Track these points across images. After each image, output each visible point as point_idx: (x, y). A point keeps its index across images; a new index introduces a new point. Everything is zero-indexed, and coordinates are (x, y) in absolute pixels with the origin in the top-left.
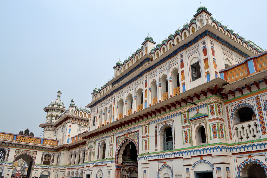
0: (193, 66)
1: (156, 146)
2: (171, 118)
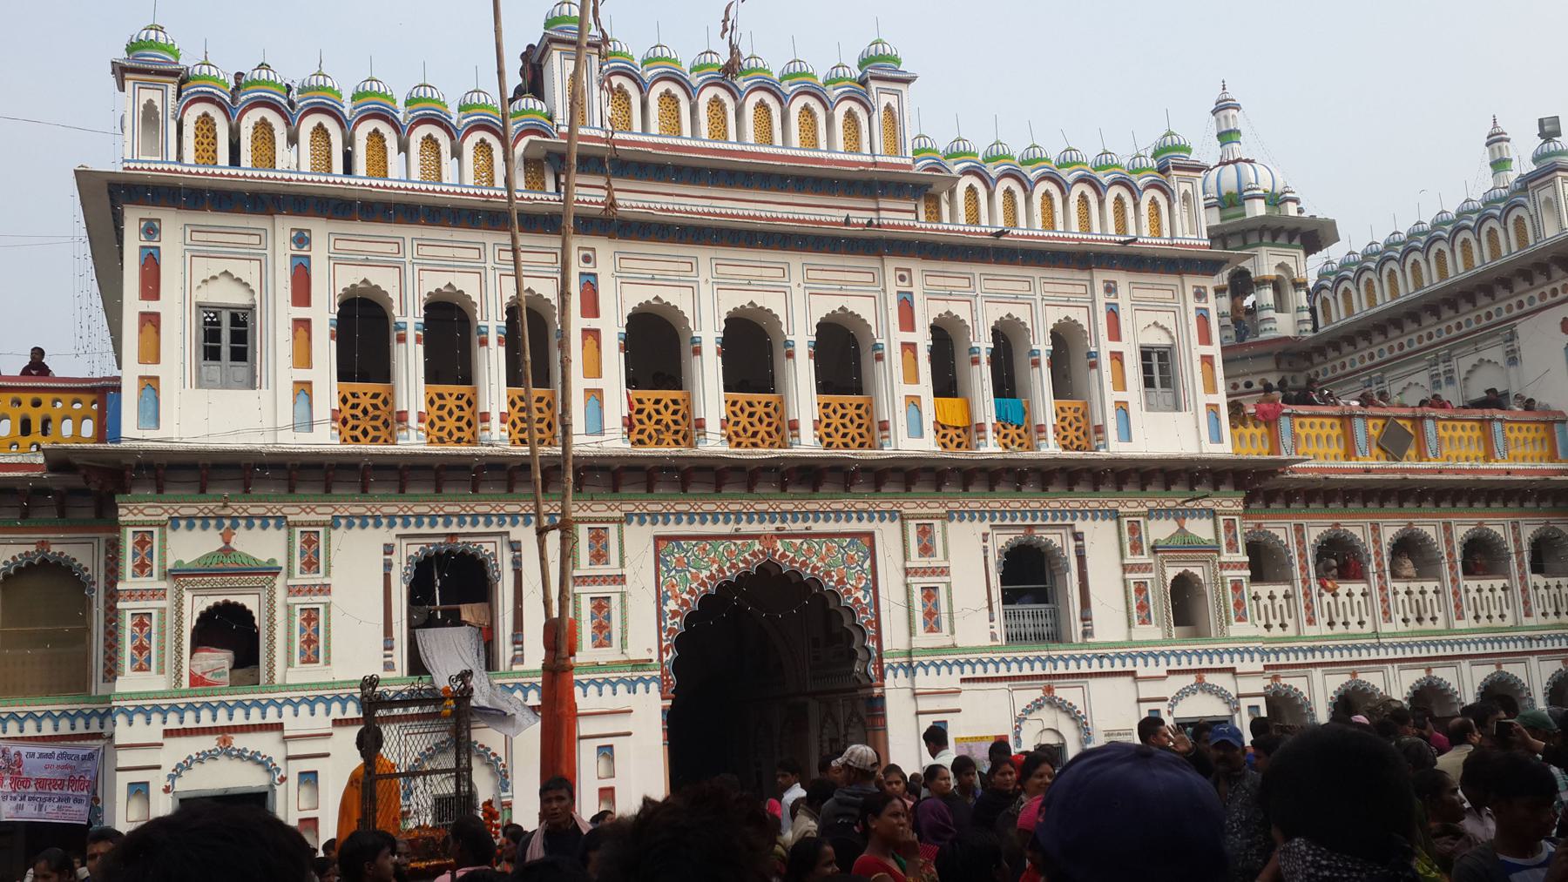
1: (992, 620)
2: (1068, 521)
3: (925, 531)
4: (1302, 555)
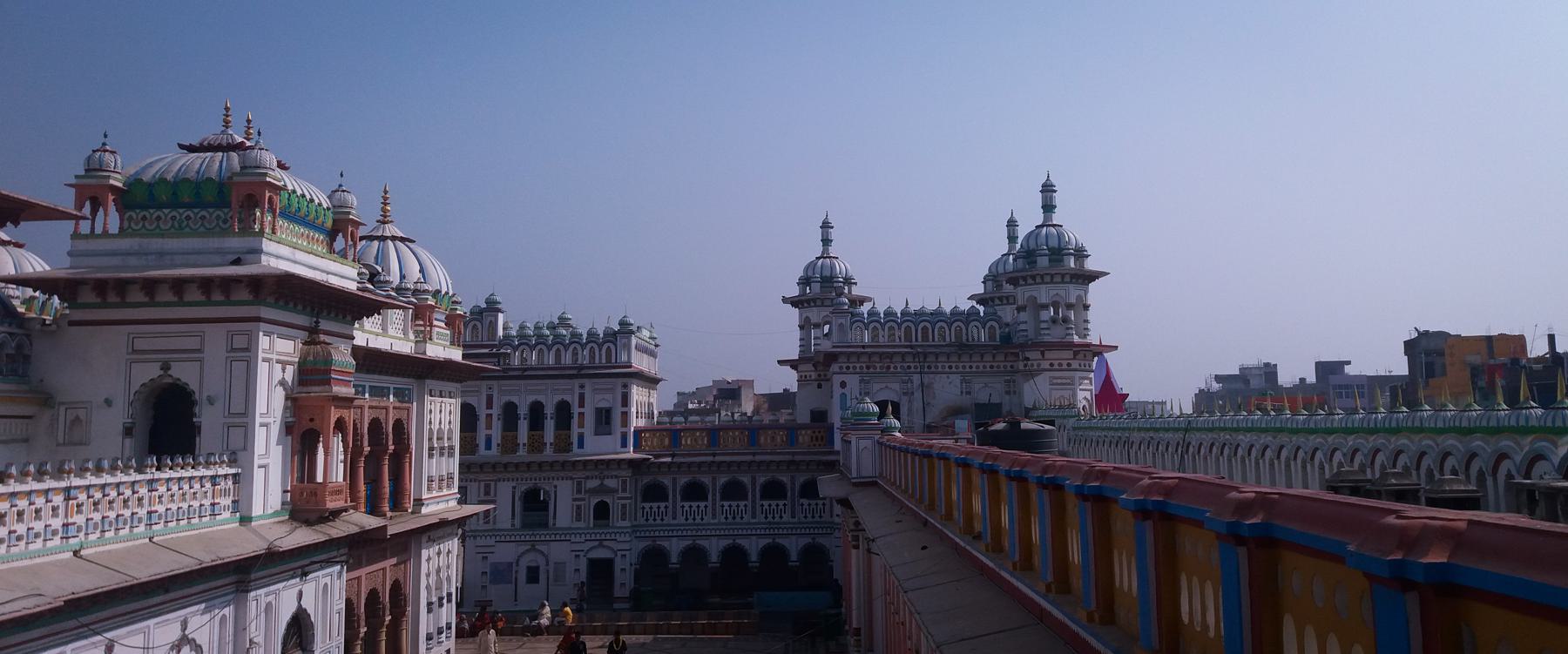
0: (599, 411)
3: (487, 487)
4: (674, 490)
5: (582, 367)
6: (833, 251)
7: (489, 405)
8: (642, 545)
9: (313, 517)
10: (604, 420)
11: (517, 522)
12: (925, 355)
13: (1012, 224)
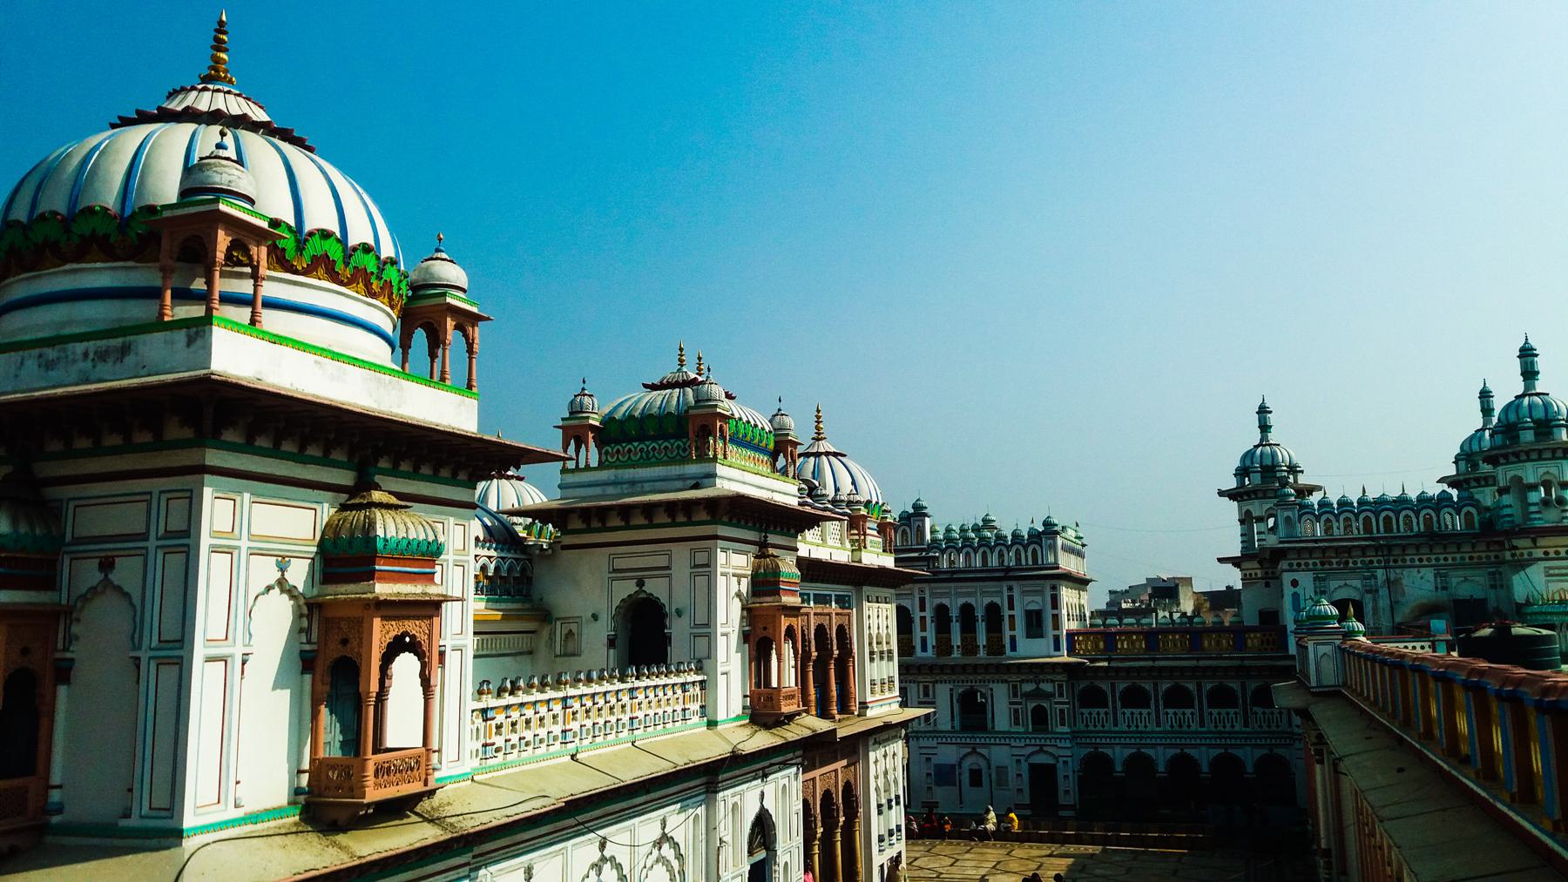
4: (1114, 696)
5: (1009, 569)
6: (1273, 437)
7: (923, 609)
8: (1084, 751)
9: (771, 721)
10: (1035, 625)
11: (957, 727)
12: (1390, 548)
13: (1485, 395)
